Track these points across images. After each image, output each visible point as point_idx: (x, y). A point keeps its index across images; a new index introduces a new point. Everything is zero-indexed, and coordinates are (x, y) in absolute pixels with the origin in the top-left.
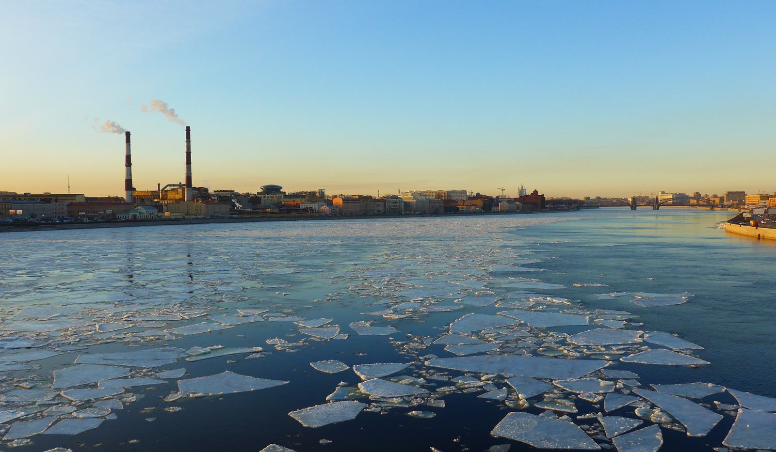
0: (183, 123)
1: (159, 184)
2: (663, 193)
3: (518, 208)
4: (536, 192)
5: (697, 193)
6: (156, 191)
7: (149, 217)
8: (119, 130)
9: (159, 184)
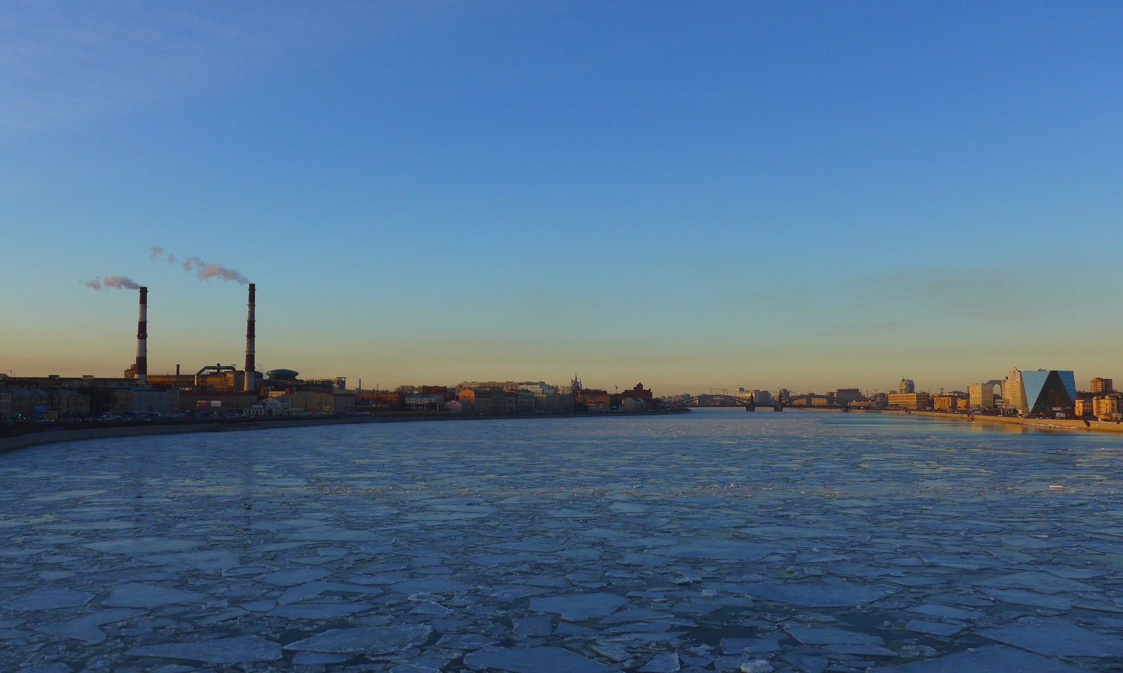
0: (242, 281)
1: (178, 366)
2: (742, 390)
3: (642, 407)
4: (640, 386)
5: (785, 390)
6: (174, 376)
7: (263, 413)
8: (128, 284)
9: (178, 366)
